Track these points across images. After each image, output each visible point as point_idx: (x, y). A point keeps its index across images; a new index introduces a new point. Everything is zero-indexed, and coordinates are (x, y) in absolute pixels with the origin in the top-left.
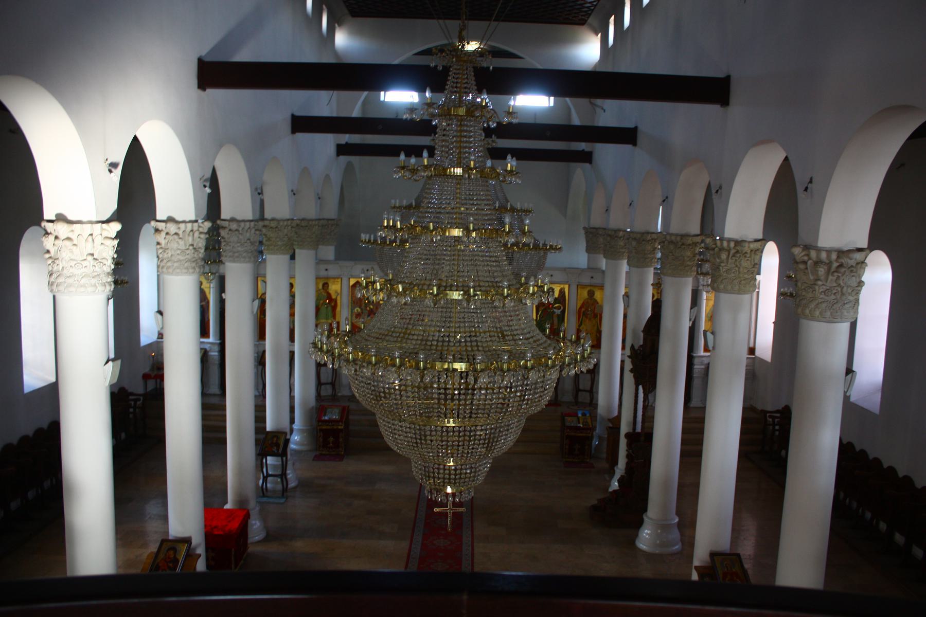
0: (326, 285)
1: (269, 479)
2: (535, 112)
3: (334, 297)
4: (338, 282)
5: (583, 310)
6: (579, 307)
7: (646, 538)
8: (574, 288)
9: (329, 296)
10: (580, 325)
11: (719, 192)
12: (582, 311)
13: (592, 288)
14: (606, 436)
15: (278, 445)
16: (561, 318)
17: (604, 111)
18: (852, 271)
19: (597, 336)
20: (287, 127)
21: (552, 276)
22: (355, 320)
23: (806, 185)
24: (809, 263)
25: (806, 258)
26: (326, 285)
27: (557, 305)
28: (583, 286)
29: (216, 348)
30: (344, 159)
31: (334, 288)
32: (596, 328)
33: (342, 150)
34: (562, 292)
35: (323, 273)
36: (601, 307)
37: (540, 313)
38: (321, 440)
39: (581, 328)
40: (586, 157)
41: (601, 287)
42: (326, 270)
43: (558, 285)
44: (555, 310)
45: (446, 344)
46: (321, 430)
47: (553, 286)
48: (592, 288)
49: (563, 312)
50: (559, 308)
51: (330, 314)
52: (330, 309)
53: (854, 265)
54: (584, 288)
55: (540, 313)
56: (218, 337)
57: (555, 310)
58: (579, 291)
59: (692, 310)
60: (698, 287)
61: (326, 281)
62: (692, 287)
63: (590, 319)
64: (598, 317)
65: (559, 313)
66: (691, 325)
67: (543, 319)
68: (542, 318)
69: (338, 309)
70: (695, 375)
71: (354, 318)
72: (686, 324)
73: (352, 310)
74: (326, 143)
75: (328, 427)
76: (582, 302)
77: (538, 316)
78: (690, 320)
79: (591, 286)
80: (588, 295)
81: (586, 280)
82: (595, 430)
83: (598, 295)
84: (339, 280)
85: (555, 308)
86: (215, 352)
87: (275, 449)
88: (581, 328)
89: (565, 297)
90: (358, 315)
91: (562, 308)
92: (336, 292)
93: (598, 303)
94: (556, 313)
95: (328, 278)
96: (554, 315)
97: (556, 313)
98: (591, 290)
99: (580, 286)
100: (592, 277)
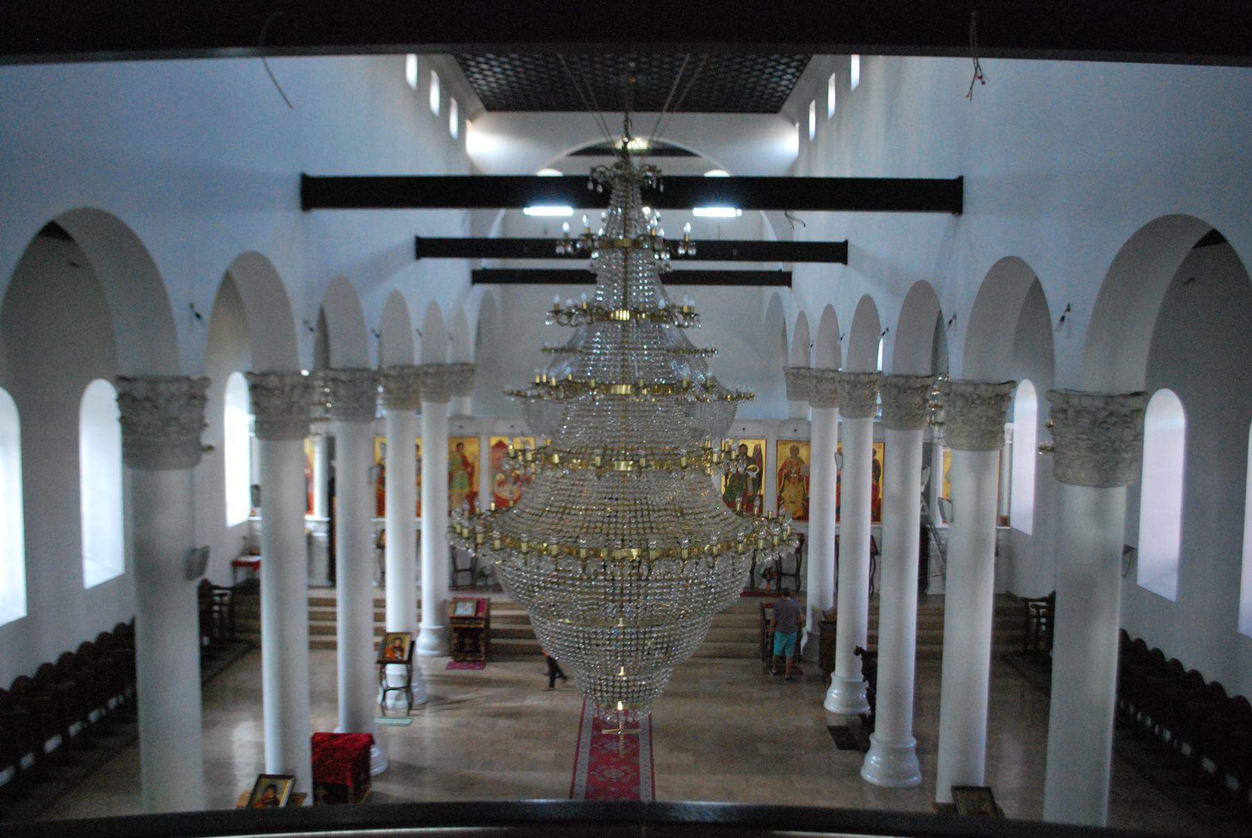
1: (390, 693)
2: (719, 223)
3: (470, 460)
4: (475, 441)
5: (785, 471)
6: (779, 469)
7: (873, 766)
9: (464, 458)
10: (781, 492)
11: (953, 323)
12: (784, 474)
13: (795, 444)
14: (819, 633)
15: (401, 649)
16: (758, 482)
17: (805, 225)
18: (1125, 422)
19: (803, 504)
20: (411, 250)
21: (744, 429)
22: (497, 490)
23: (1062, 314)
24: (1070, 411)
25: (1065, 406)
26: (461, 447)
27: (751, 466)
28: (785, 442)
29: (324, 528)
30: (480, 288)
31: (470, 449)
32: (802, 494)
33: (479, 277)
34: (758, 451)
35: (457, 431)
36: (808, 468)
37: (730, 477)
38: (455, 641)
39: (783, 495)
40: (784, 279)
41: (808, 443)
42: (461, 427)
43: (753, 441)
44: (749, 473)
45: (613, 526)
46: (456, 630)
47: (747, 443)
48: (795, 444)
49: (760, 474)
51: (466, 482)
52: (466, 476)
53: (1128, 413)
54: (785, 444)
55: (730, 477)
56: (326, 513)
57: (749, 473)
58: (779, 448)
59: (924, 471)
60: (933, 440)
61: (461, 441)
62: (924, 440)
63: (794, 483)
64: (805, 480)
65: (755, 477)
66: (923, 490)
67: (733, 484)
68: (734, 482)
70: (931, 554)
71: (496, 487)
72: (917, 489)
73: (494, 477)
74: (459, 268)
75: (464, 626)
76: (783, 462)
77: (728, 480)
78: (922, 484)
79: (794, 441)
80: (791, 452)
81: (788, 434)
82: (805, 625)
83: (803, 453)
84: (476, 439)
86: (321, 532)
87: (398, 654)
88: (783, 495)
89: (761, 456)
90: (501, 483)
91: (758, 470)
92: (473, 454)
93: (803, 463)
94: (751, 477)
95: (462, 437)
96: (749, 479)
97: (751, 477)
98: (794, 446)
100: (795, 430)
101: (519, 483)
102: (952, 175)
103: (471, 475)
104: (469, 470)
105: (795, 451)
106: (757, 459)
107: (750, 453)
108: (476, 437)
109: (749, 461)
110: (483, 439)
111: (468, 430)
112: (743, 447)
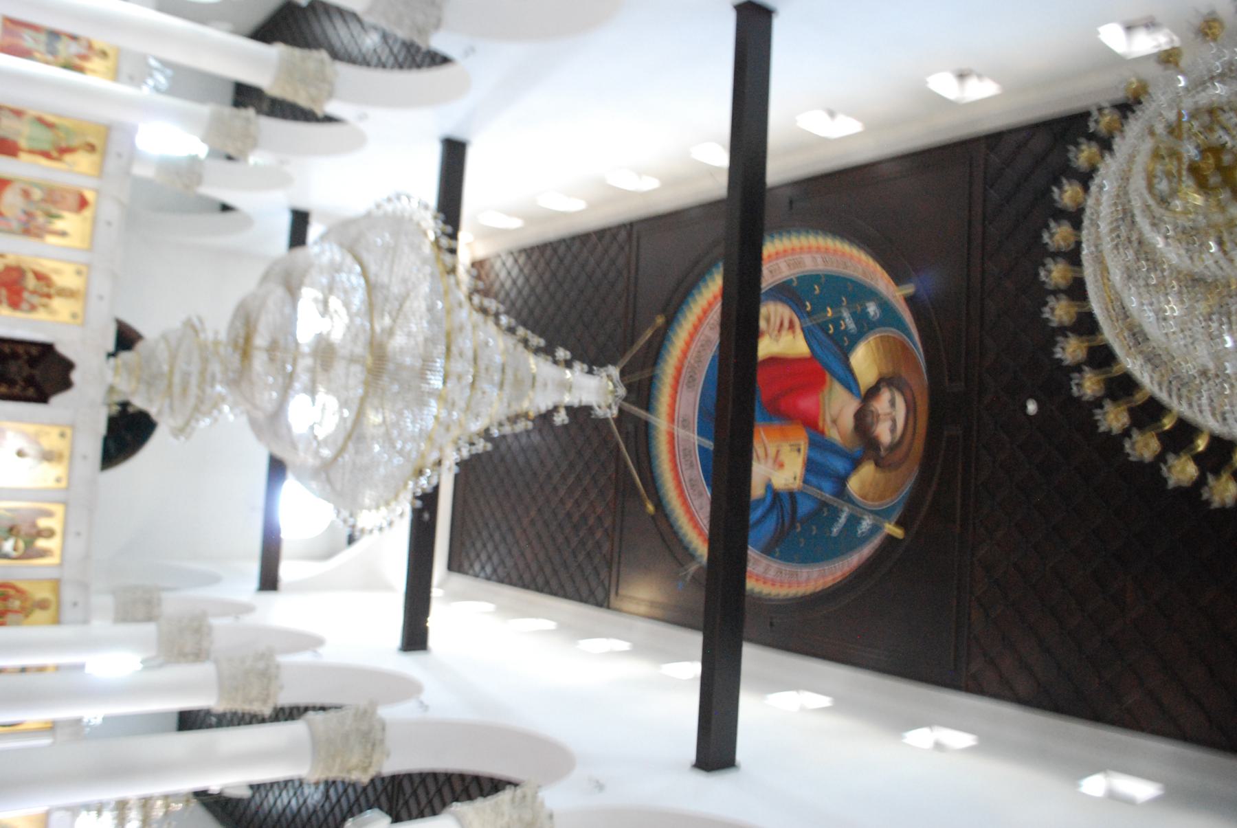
0: (91, 148)
3: (68, 158)
5: (12, 592)
8: (54, 574)
31: (82, 162)
34: (43, 553)
36: (18, 624)
41: (57, 621)
50: (15, 549)
52: (46, 147)
69: (43, 162)
81: (68, 595)
83: (38, 615)
85: (16, 543)
90: (26, 194)
95: (104, 155)
99: (56, 584)
101: (24, 218)
102: (740, 756)
103: (46, 155)
104: (55, 154)
105: (43, 605)
106: (30, 553)
107: (41, 543)
108: (101, 172)
109: (29, 543)
110: (93, 183)
111: (112, 165)
112: (50, 533)
